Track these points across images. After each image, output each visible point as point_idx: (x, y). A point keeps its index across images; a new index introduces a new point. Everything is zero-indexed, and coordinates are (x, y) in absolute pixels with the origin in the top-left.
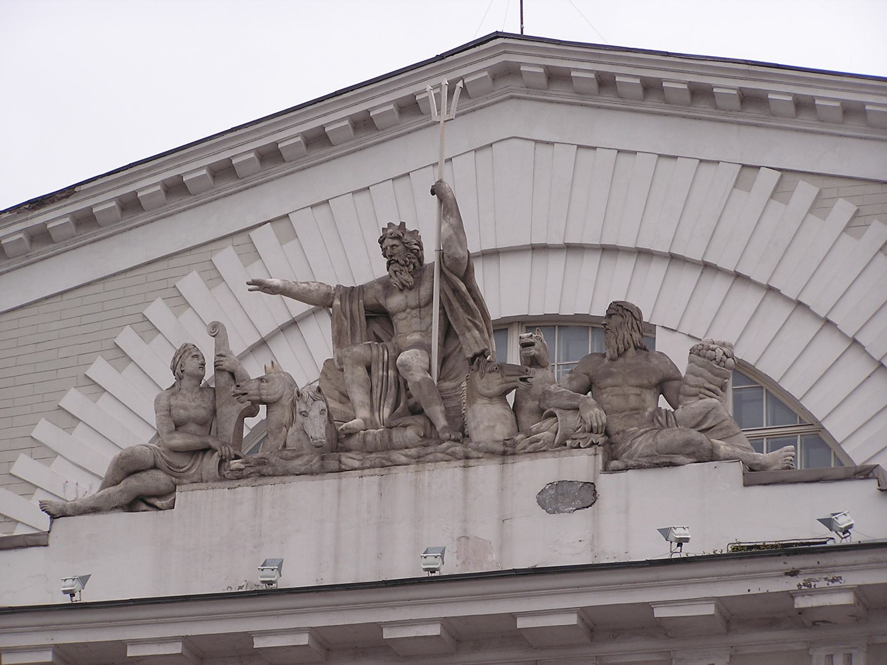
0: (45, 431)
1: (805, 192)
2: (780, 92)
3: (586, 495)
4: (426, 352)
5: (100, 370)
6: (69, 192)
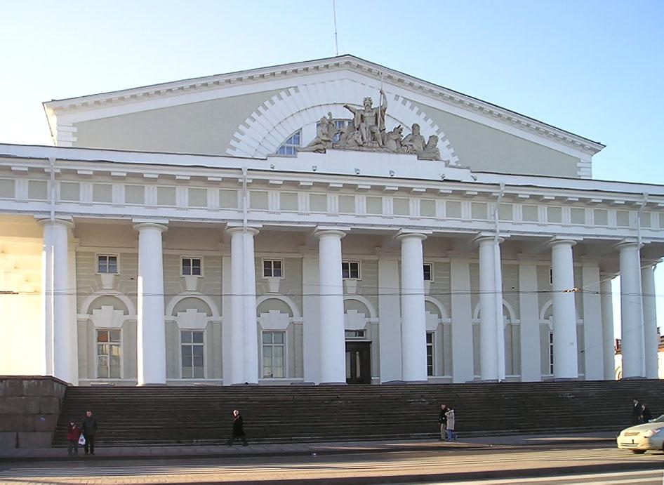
0: (241, 127)
1: (408, 104)
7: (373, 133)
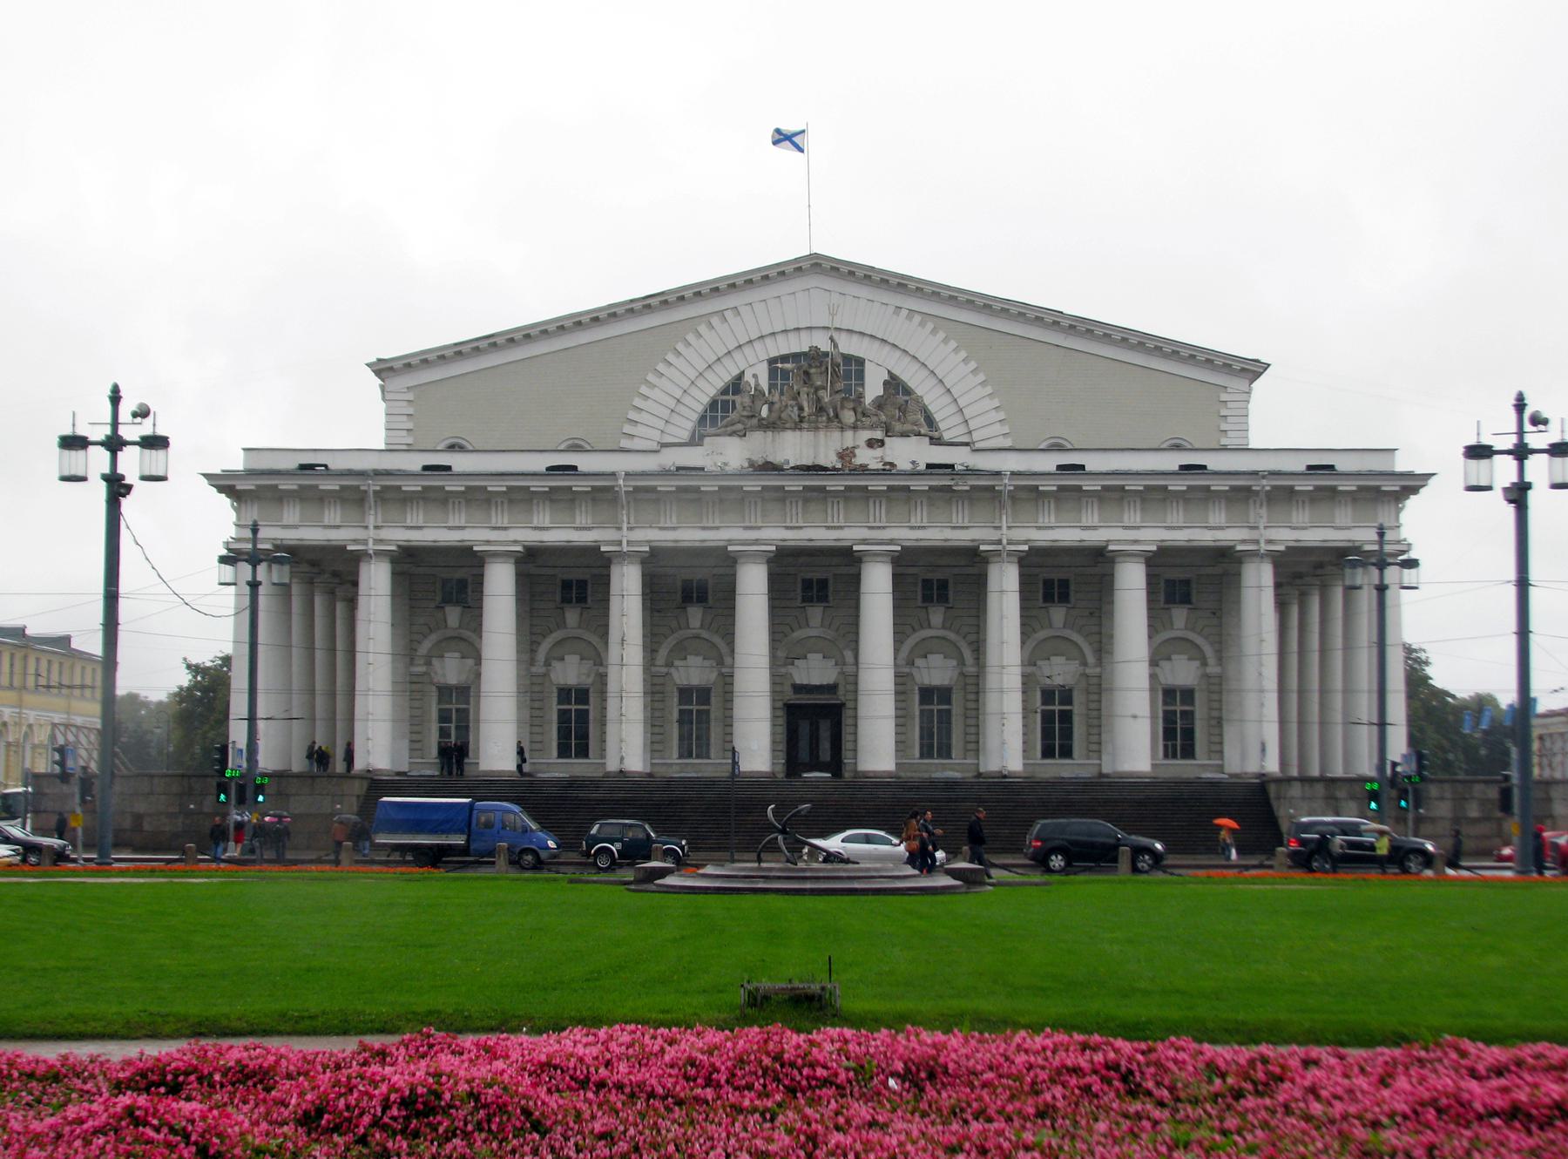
0: (651, 377)
1: (917, 318)
2: (912, 285)
3: (882, 443)
4: (817, 383)
5: (670, 357)
6: (662, 293)
7: (819, 400)
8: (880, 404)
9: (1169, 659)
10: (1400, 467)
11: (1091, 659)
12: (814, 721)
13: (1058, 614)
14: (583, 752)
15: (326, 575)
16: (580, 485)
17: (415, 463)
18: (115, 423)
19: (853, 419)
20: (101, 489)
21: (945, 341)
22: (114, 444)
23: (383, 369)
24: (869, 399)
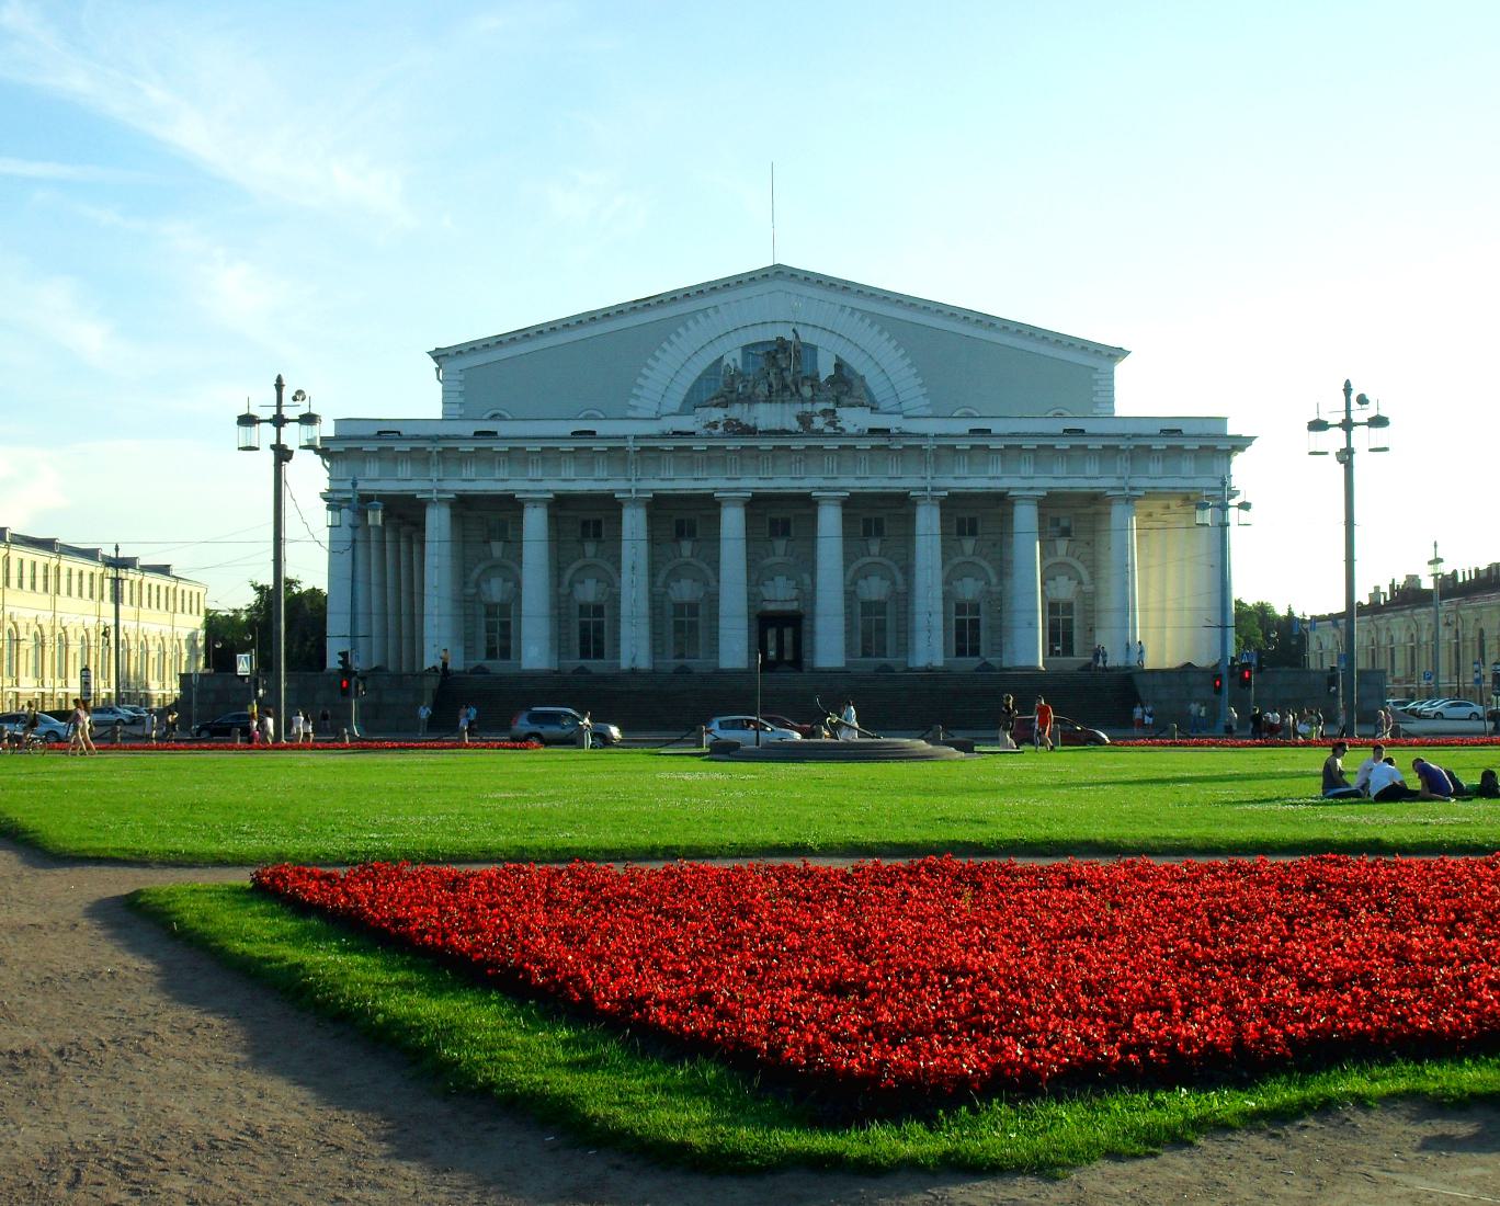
1: (858, 315)
4: (780, 366)
7: (783, 379)
8: (830, 380)
9: (1054, 579)
10: (1231, 430)
11: (994, 580)
12: (781, 630)
13: (969, 544)
14: (599, 654)
15: (405, 514)
16: (597, 445)
17: (468, 429)
18: (279, 405)
19: (810, 394)
20: (270, 456)
21: (880, 333)
22: (279, 421)
23: (439, 356)
24: (823, 379)
